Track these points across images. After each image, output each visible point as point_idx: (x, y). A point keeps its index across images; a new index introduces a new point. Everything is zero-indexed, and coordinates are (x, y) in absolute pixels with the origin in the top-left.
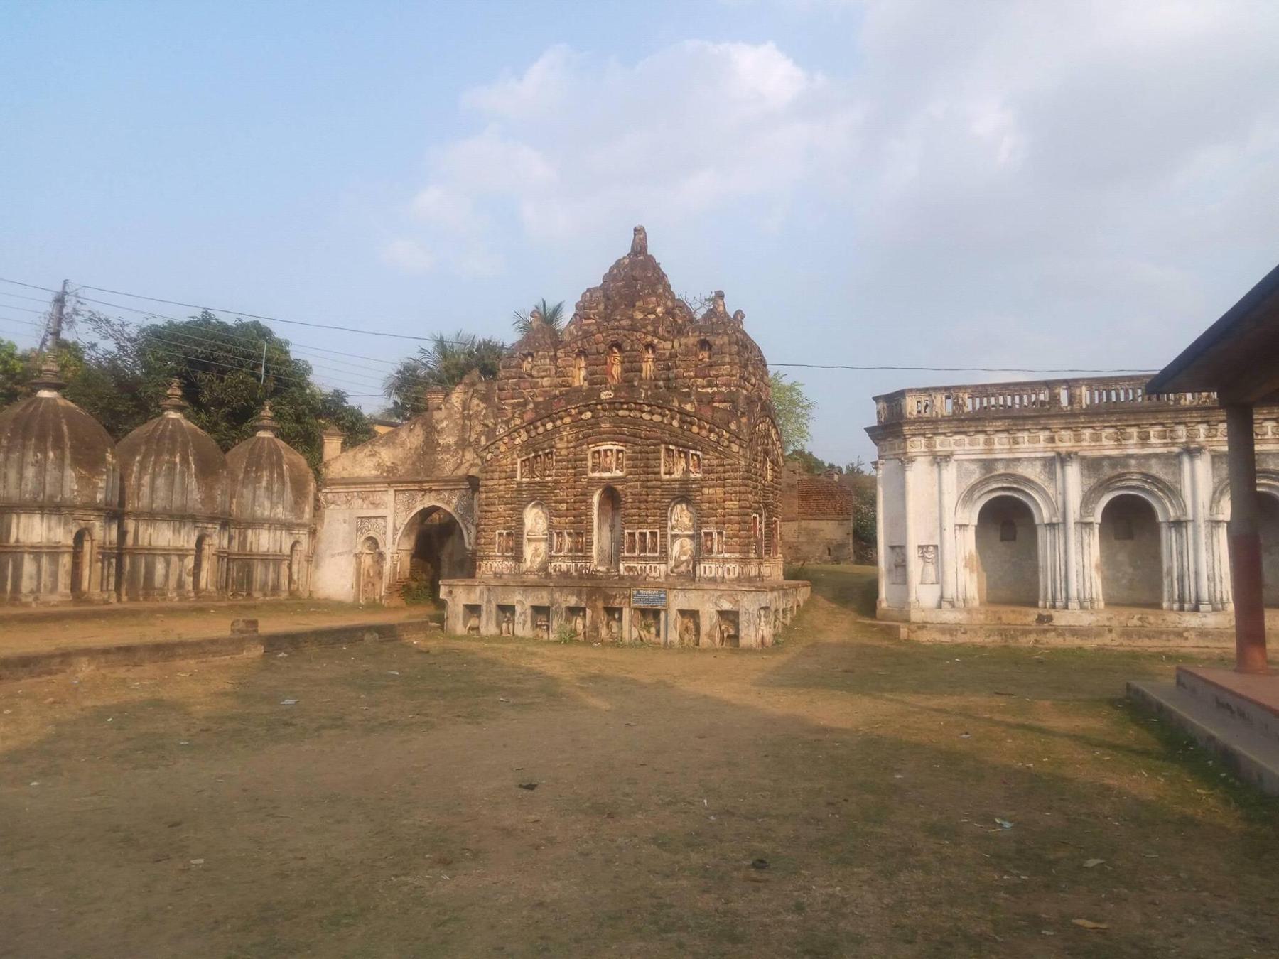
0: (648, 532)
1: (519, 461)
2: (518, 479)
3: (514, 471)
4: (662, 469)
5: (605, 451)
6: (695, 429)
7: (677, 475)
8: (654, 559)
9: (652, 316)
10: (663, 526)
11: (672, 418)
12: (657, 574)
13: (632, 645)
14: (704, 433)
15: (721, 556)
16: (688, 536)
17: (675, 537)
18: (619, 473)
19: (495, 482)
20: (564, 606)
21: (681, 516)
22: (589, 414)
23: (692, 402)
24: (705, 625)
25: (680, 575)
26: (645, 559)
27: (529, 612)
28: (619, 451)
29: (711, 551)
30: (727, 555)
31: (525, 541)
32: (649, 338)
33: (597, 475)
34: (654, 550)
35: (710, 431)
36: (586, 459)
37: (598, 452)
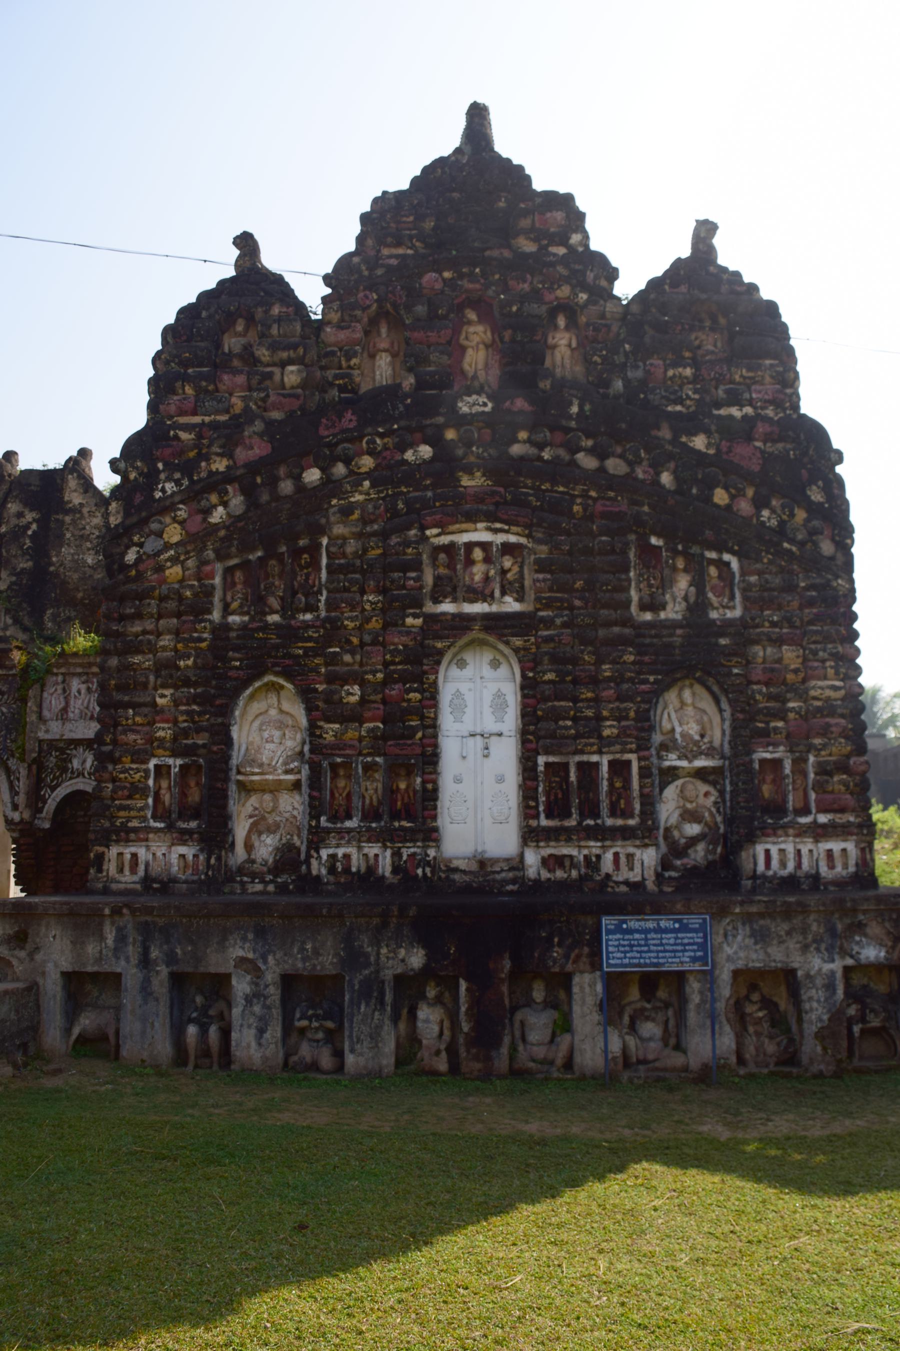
0: (605, 761)
1: (219, 567)
2: (216, 616)
3: (209, 592)
4: (634, 595)
5: (470, 546)
6: (720, 497)
7: (673, 612)
8: (626, 834)
9: (561, 251)
10: (643, 746)
11: (657, 467)
12: (635, 876)
13: (606, 1080)
14: (744, 507)
15: (803, 820)
16: (701, 774)
18: (511, 605)
19: (149, 625)
20: (388, 974)
21: (689, 716)
22: (426, 451)
23: (708, 432)
24: (816, 1010)
25: (693, 872)
26: (601, 834)
27: (274, 993)
28: (507, 549)
29: (777, 809)
30: (823, 819)
31: (233, 788)
32: (564, 292)
33: (447, 607)
35: (760, 503)
36: (417, 565)
37: (450, 549)
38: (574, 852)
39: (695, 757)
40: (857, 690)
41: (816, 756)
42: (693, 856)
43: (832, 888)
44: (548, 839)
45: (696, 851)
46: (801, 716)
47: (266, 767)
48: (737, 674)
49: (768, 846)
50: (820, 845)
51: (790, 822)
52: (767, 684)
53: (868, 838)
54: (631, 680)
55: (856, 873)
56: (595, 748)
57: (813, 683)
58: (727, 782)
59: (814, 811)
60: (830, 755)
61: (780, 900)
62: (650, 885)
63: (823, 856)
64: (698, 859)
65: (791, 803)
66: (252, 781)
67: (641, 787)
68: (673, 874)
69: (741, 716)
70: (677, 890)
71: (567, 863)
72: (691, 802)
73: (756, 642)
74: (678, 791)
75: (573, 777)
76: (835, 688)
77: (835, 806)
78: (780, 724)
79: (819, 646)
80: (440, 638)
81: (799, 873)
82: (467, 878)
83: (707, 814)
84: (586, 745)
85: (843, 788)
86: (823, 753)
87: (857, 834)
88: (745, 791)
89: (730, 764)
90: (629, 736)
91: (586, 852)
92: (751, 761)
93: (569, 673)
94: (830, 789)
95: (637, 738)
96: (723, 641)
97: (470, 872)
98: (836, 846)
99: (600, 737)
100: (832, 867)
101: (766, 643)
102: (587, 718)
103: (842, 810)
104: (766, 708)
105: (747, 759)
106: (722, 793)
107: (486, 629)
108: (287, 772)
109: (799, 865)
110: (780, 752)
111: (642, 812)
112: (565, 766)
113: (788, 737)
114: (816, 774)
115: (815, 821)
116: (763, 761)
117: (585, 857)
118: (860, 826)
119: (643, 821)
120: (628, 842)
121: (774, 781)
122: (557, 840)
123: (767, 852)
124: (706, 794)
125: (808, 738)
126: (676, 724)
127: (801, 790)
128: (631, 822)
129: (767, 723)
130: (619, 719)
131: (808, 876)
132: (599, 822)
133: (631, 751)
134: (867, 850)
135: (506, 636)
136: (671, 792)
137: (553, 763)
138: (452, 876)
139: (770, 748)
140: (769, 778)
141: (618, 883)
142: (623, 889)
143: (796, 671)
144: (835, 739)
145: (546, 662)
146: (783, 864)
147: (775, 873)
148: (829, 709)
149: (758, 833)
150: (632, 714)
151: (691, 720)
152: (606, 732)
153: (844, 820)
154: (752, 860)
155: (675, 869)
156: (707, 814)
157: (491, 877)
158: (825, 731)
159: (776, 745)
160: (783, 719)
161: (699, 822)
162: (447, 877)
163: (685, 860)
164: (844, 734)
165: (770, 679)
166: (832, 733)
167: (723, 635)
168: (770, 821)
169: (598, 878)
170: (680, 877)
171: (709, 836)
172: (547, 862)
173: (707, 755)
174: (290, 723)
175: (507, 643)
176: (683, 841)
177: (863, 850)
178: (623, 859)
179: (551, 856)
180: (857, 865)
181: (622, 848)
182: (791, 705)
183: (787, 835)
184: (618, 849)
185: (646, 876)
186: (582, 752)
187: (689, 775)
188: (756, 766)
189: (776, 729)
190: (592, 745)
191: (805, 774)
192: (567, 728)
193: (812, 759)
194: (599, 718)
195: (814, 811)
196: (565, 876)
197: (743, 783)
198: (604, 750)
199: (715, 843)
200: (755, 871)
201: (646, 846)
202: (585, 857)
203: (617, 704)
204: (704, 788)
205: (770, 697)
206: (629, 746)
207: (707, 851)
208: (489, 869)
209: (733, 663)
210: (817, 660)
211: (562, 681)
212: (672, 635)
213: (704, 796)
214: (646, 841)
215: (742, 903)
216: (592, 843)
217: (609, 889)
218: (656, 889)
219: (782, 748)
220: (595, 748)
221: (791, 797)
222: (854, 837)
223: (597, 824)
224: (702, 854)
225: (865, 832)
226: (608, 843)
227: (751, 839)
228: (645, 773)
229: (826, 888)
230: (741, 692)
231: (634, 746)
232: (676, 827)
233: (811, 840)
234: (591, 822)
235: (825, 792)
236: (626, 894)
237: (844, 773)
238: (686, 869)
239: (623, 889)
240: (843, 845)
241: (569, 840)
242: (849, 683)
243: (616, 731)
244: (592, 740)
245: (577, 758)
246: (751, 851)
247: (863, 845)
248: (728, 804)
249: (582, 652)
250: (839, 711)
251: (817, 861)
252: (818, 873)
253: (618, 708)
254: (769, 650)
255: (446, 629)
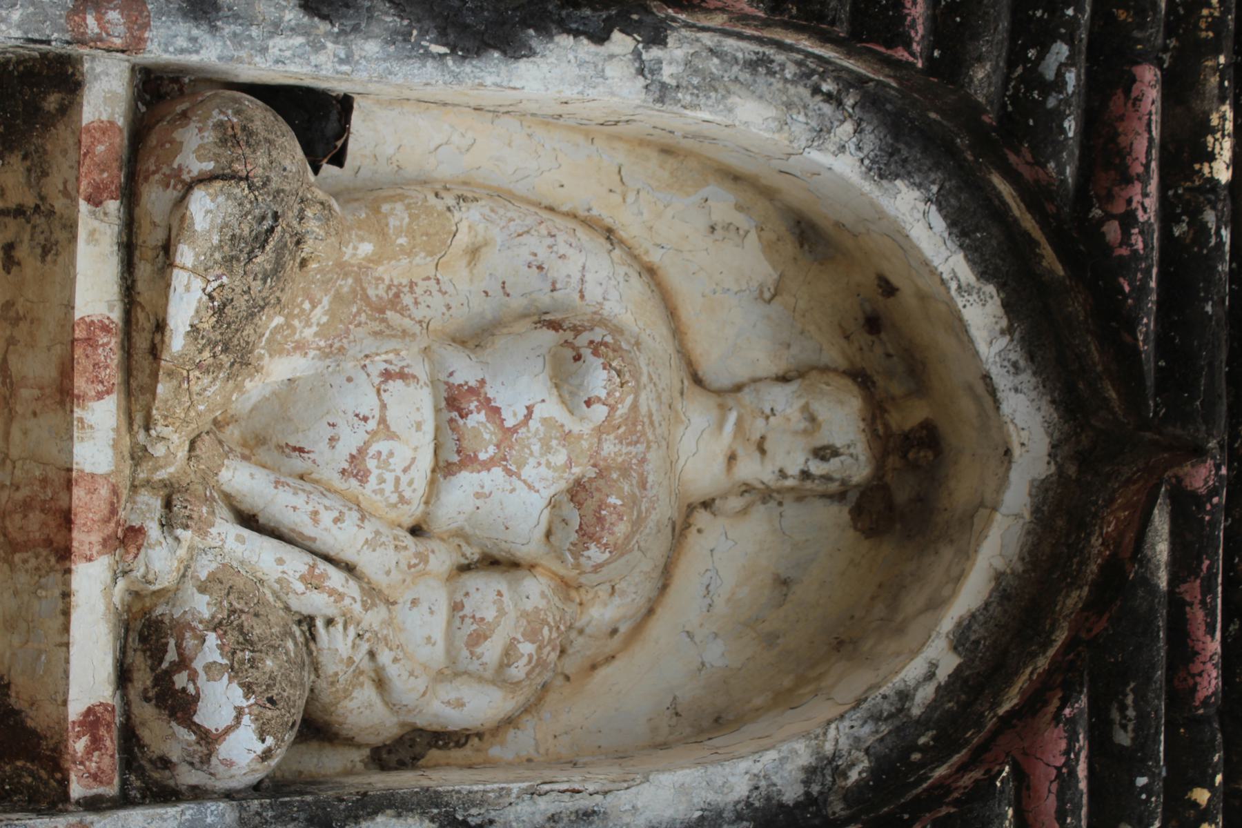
47: (209, 393)
66: (56, 244)
108: (147, 635)
174: (603, 612)
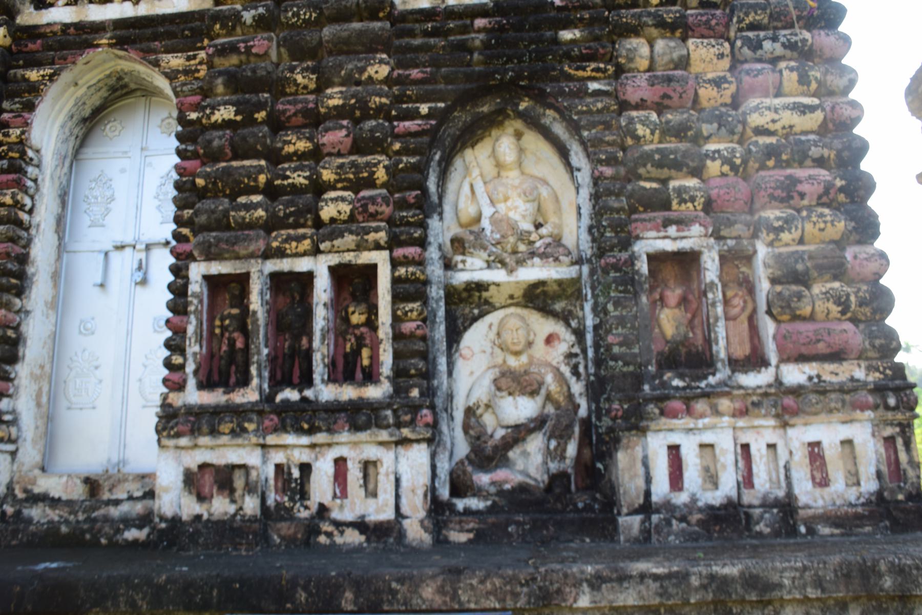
0: (320, 268)
8: (359, 416)
12: (379, 510)
15: (752, 380)
16: (537, 298)
17: (468, 303)
26: (308, 418)
30: (794, 375)
34: (346, 369)
38: (252, 458)
39: (520, 262)
40: (848, 112)
41: (771, 244)
42: (520, 465)
43: (825, 530)
44: (195, 431)
45: (525, 454)
46: (734, 168)
48: (597, 93)
49: (675, 439)
50: (791, 432)
51: (723, 383)
52: (660, 108)
53: (899, 416)
54: (382, 111)
55: (879, 494)
56: (306, 244)
57: (753, 102)
58: (588, 307)
59: (774, 360)
60: (801, 241)
61: (698, 573)
62: (415, 530)
63: (800, 457)
64: (533, 471)
65: (722, 343)
67: (396, 320)
68: (474, 503)
69: (608, 171)
70: (480, 536)
71: (239, 482)
72: (517, 354)
73: (635, 31)
74: (492, 335)
75: (256, 302)
76: (804, 109)
77: (821, 348)
78: (692, 183)
79: (762, 34)
80: (37, 64)
81: (749, 498)
82: (54, 515)
83: (549, 378)
84: (289, 239)
85: (835, 309)
86: (785, 236)
87: (875, 407)
88: (621, 321)
89: (592, 272)
90: (374, 216)
91: (279, 457)
92: (632, 259)
93: (260, 106)
94: (807, 311)
95: (390, 221)
96: (567, 35)
97: (70, 503)
98: (828, 432)
99: (318, 223)
100: (823, 482)
101: (654, 32)
102: (295, 190)
103: (837, 356)
104: (658, 151)
105: (624, 256)
106: (579, 334)
107: (121, 43)
109: (748, 480)
110: (693, 238)
111: (399, 373)
112: (243, 280)
113: (708, 206)
114: (774, 281)
115: (778, 382)
116: (655, 259)
117: (279, 467)
118: (879, 390)
119: (399, 390)
120: (363, 436)
121: (684, 301)
122: (214, 432)
123: (674, 451)
124: (549, 340)
125: (751, 212)
126: (484, 201)
127: (744, 317)
128: (375, 392)
129: (664, 182)
130: (355, 186)
131: (766, 504)
132: (309, 393)
133: (378, 247)
134: (900, 441)
135: (155, 52)
136: (476, 337)
137: (220, 276)
138: (26, 512)
139: (672, 230)
140: (674, 294)
141: (340, 525)
142: (353, 537)
143: (718, 83)
144: (809, 208)
145: (220, 89)
146: (711, 478)
147: (694, 499)
148: (789, 151)
149: (652, 408)
150: (381, 175)
151: (513, 194)
152: (328, 212)
153: (843, 378)
154: (641, 470)
155: (477, 492)
156: (549, 378)
157: (101, 512)
158: (788, 193)
159: (681, 223)
160: (697, 172)
161: (533, 393)
162: (18, 513)
163: (501, 474)
164: (826, 199)
165: (666, 96)
166: (802, 195)
167: (567, 25)
168: (676, 382)
169: (304, 514)
170: (491, 510)
171: (553, 425)
172: (202, 480)
173: (544, 256)
175: (156, 64)
176: (500, 433)
177: (889, 441)
178: (354, 474)
179: (203, 467)
180: (879, 475)
181: (356, 447)
182: (711, 147)
183: (717, 412)
184: (343, 451)
185: (405, 509)
186: (281, 254)
187: (512, 301)
188: (643, 267)
189: (680, 191)
190: (299, 239)
191: (750, 288)
192: (249, 207)
193: (762, 251)
194: (318, 188)
195: (774, 360)
196: (232, 509)
197: (617, 304)
198: (322, 247)
199: (561, 434)
200: (648, 494)
201: (404, 442)
202: (279, 467)
203: (353, 158)
204: (543, 326)
205: (667, 131)
206: (372, 237)
207: (548, 454)
208: (106, 496)
209: (588, 73)
210: (760, 60)
211: (249, 121)
212: (466, 29)
213: (548, 346)
214: (406, 432)
215: (596, 583)
216: (290, 439)
217: (322, 539)
218: (427, 538)
219: (696, 229)
220: (306, 244)
221: (721, 330)
222: (869, 414)
223: (304, 400)
224: (537, 459)
225: (892, 401)
226: (321, 438)
227: (636, 422)
228: (409, 290)
229: (811, 531)
230: (608, 126)
231: (382, 236)
232: (488, 406)
233: (772, 422)
234: (290, 395)
235: (796, 318)
236: (358, 549)
237: (835, 278)
238: (501, 493)
239: (353, 537)
240: (845, 432)
241: (238, 432)
242: (828, 103)
243: (346, 208)
244: (301, 231)
245: (272, 266)
246: (639, 452)
247: (889, 431)
248: (591, 353)
249: (292, 69)
250: (815, 152)
251: (787, 469)
252: (790, 494)
253: (353, 164)
254: (660, 45)
255: (50, 48)
